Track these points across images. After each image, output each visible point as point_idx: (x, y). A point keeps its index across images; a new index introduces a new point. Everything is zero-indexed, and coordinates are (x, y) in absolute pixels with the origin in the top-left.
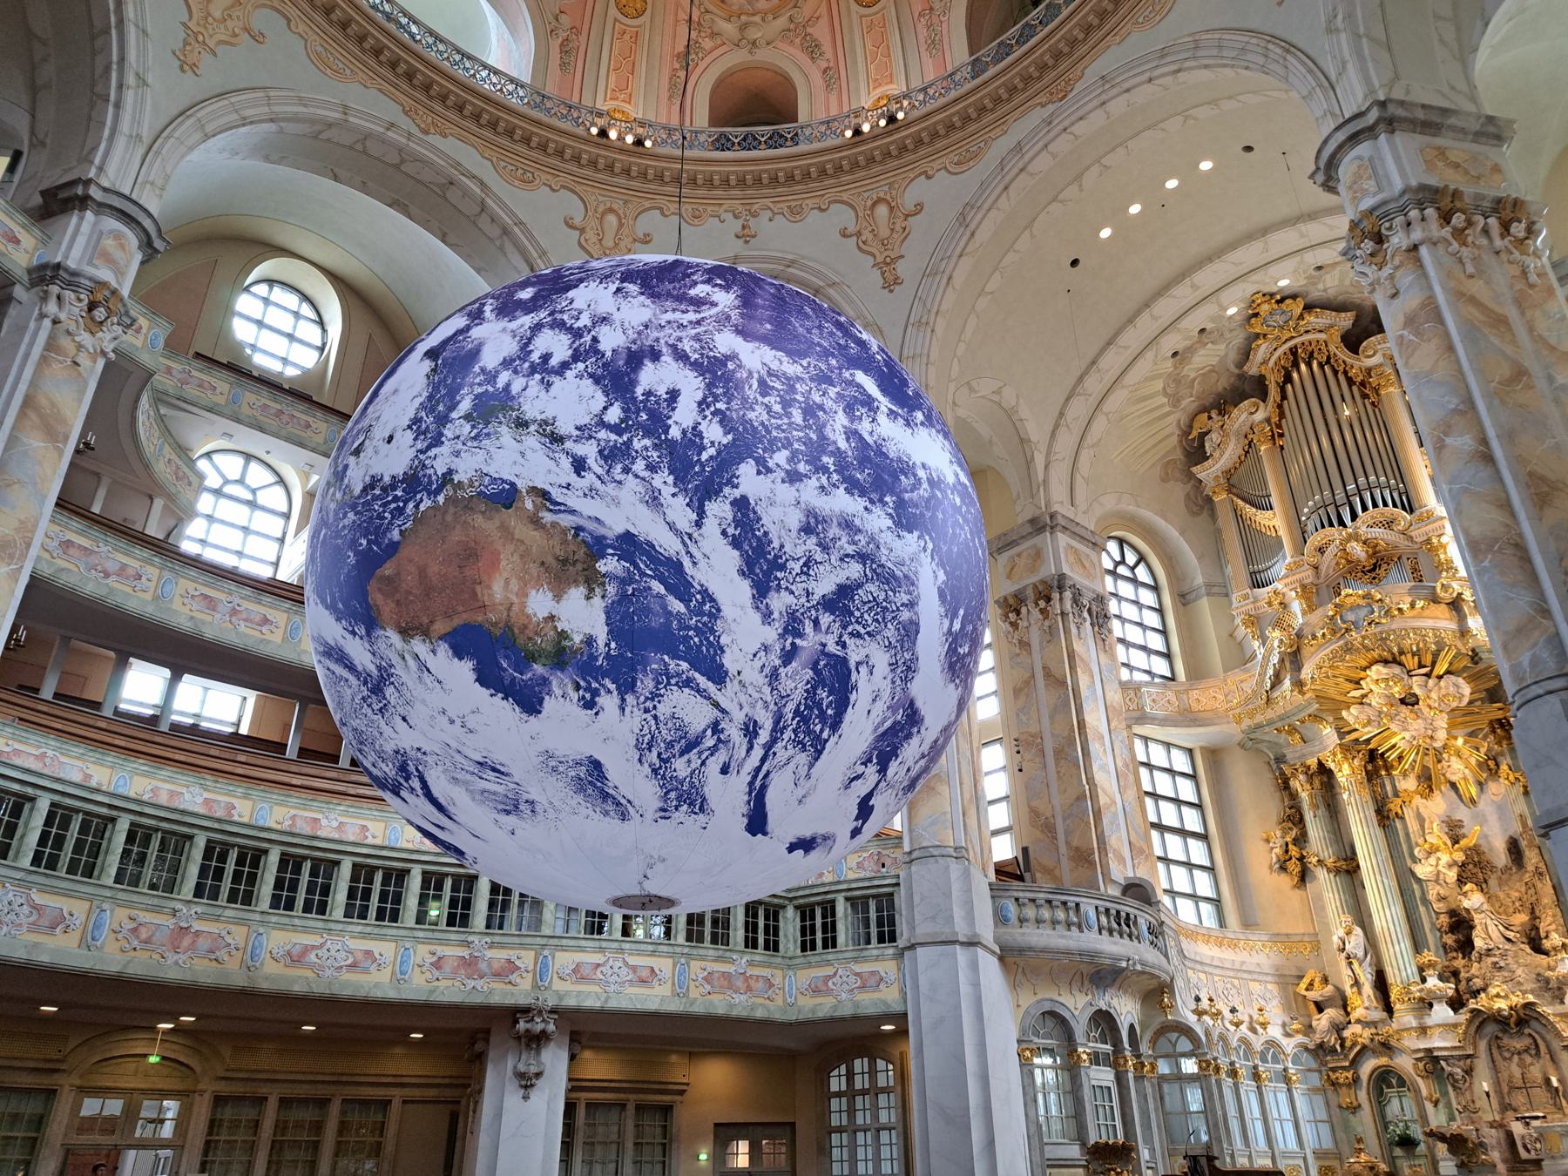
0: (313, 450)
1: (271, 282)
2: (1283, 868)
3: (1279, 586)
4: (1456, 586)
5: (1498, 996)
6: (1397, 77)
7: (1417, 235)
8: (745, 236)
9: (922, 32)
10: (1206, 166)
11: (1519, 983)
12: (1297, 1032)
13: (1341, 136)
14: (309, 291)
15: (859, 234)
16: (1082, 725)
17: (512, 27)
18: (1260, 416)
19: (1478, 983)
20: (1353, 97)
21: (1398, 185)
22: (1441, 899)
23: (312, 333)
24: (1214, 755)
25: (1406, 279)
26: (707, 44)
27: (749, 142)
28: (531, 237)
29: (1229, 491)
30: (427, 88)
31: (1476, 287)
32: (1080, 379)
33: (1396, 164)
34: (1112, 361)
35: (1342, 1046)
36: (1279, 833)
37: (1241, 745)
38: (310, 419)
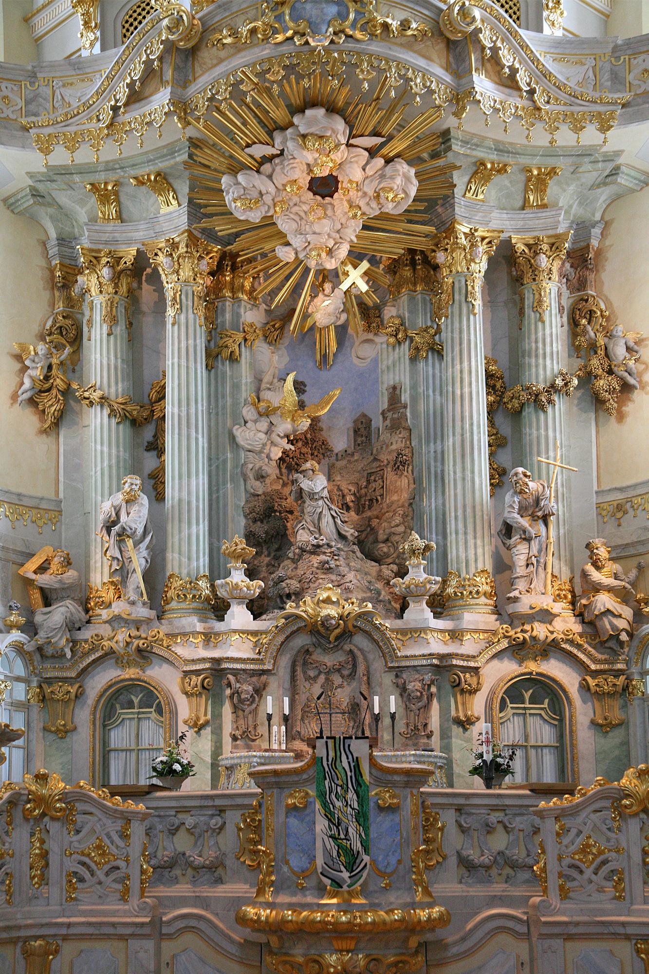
11: (348, 590)
36: (42, 348)
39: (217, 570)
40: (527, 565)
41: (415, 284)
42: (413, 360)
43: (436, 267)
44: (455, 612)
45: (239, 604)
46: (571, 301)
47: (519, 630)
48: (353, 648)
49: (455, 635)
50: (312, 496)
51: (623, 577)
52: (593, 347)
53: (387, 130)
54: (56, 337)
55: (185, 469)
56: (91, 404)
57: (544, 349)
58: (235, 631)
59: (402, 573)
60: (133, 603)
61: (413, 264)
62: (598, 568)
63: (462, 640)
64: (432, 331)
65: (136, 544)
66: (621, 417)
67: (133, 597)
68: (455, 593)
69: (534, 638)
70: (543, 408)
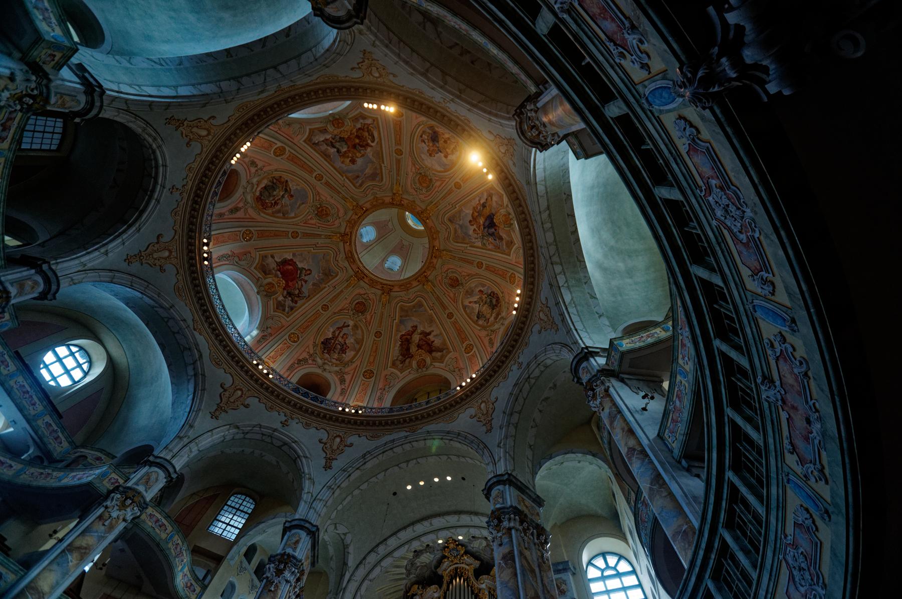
0: (24, 416)
1: (81, 348)
6: (514, 470)
7: (512, 524)
8: (284, 424)
9: (379, 394)
10: (449, 478)
13: (495, 480)
14: (94, 358)
15: (325, 444)
17: (250, 323)
18: (436, 595)
20: (501, 469)
21: (509, 503)
23: (77, 374)
25: (506, 540)
26: (310, 362)
27: (306, 395)
28: (204, 382)
30: (207, 318)
31: (527, 553)
32: (378, 546)
33: (511, 497)
34: (393, 542)
38: (38, 402)
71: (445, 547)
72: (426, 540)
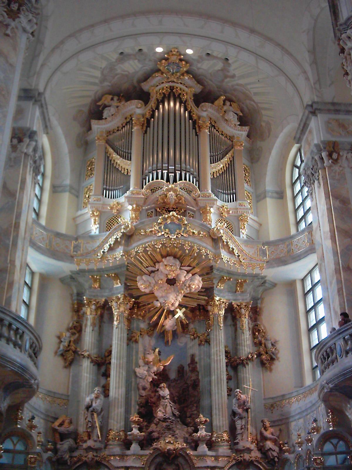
2: (62, 355)
3: (122, 199)
4: (222, 231)
5: (169, 442)
11: (176, 438)
12: (50, 450)
16: (17, 226)
19: (156, 435)
22: (144, 389)
24: (45, 279)
29: (107, 142)
32: (81, 30)
34: (101, 33)
35: (71, 462)
36: (68, 334)
37: (62, 280)
39: (128, 428)
40: (241, 429)
41: (200, 317)
42: (200, 345)
43: (207, 311)
44: (216, 448)
45: (136, 442)
46: (252, 326)
47: (239, 456)
48: (178, 463)
49: (217, 458)
50: (163, 397)
51: (274, 434)
52: (260, 343)
53: (194, 264)
54: (73, 330)
55: (117, 385)
56: (84, 357)
57: (244, 344)
58: (134, 455)
59: (196, 431)
60: (95, 441)
61: (200, 310)
62: (266, 430)
63: (219, 461)
64: (206, 335)
65: (98, 415)
66: (271, 370)
67: (95, 438)
68: (216, 440)
69: (245, 460)
70: (244, 366)
71: (163, 58)
72: (143, 42)
